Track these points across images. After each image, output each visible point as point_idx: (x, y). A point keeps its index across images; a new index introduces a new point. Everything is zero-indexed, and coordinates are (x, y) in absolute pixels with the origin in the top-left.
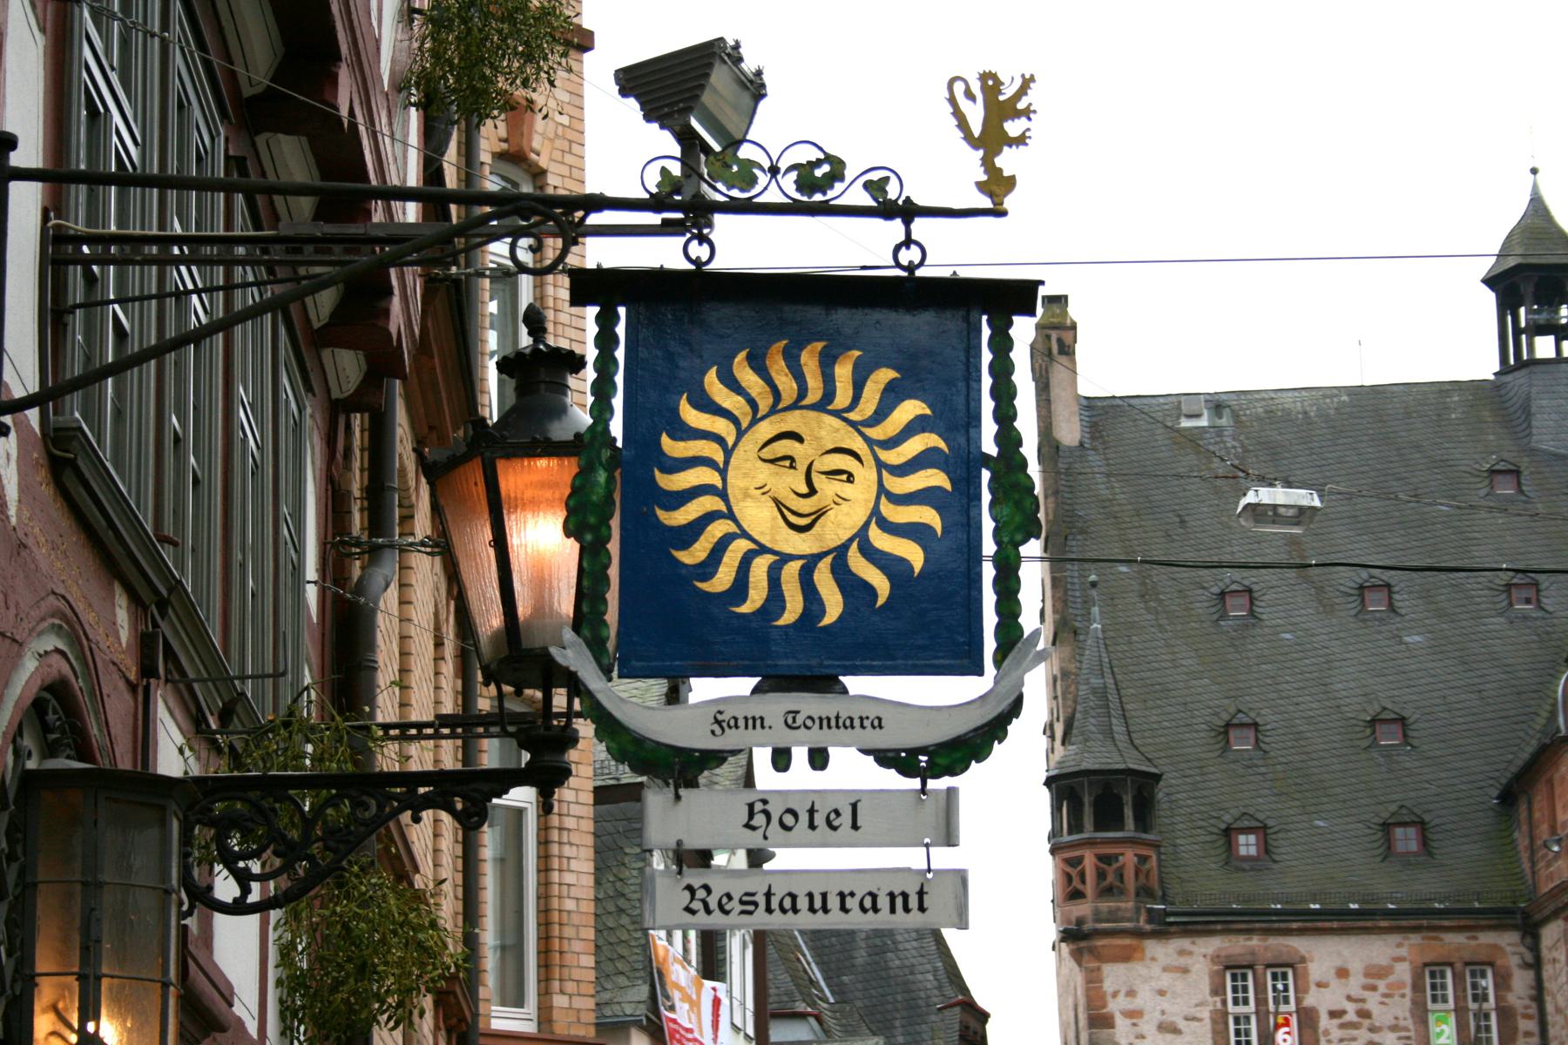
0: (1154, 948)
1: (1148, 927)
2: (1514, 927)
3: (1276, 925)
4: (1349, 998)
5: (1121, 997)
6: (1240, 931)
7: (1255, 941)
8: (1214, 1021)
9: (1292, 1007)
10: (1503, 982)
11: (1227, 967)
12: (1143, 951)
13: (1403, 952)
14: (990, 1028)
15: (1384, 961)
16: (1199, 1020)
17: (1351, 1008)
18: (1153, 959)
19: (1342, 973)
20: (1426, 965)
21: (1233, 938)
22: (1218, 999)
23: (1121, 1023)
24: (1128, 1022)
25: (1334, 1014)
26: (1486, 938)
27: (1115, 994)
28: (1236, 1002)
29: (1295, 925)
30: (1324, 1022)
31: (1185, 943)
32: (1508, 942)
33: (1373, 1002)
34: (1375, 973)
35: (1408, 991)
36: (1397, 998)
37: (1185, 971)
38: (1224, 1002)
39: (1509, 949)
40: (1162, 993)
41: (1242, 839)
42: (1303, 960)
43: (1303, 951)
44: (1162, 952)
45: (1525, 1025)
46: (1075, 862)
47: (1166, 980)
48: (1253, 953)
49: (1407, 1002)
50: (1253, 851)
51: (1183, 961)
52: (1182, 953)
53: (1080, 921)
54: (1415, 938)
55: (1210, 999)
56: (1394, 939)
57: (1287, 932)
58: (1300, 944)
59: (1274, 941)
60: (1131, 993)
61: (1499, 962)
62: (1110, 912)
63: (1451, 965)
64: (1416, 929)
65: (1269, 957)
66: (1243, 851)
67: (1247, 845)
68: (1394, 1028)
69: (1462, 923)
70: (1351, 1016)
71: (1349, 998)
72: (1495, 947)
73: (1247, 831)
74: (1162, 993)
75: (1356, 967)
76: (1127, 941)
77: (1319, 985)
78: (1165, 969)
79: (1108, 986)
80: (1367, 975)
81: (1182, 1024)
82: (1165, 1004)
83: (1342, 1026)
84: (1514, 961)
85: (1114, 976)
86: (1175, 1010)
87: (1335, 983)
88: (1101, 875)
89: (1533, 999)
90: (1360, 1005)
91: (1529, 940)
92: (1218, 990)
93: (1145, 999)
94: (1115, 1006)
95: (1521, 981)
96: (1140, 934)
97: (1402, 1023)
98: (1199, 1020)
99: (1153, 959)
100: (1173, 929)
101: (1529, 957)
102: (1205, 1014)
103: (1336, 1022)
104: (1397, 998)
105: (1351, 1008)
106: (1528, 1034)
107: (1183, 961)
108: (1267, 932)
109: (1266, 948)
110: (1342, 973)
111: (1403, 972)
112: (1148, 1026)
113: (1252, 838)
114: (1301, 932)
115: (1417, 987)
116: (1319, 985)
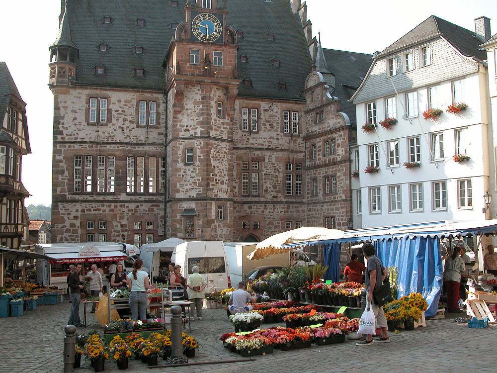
0: (72, 91)
1: (71, 86)
2: (162, 93)
3: (104, 88)
4: (120, 107)
5: (62, 103)
6: (95, 89)
7: (98, 92)
8: (86, 110)
9: (106, 109)
10: (158, 106)
11: (91, 98)
12: (69, 92)
13: (134, 97)
14: (27, 107)
15: (129, 99)
16: (82, 110)
17: (120, 110)
18: (72, 94)
19: (119, 101)
20: (140, 101)
21: (92, 90)
22: (87, 105)
23: (61, 108)
24: (64, 109)
25: (116, 111)
26: (155, 95)
27: (61, 102)
28: (92, 106)
29: (108, 88)
30: (113, 112)
31: (80, 91)
32: (160, 96)
33: (126, 109)
34: (127, 101)
35: (135, 107)
36: (132, 108)
37: (80, 98)
38: (89, 106)
39: (160, 98)
40: (73, 103)
41: (99, 69)
42: (110, 97)
43: (110, 95)
44: (75, 92)
45: (162, 116)
46: (53, 69)
47: (74, 100)
48: (97, 94)
49: (134, 109)
50: (102, 73)
51: (79, 95)
52: (79, 93)
53: (53, 83)
54: (138, 94)
55: (85, 105)
56: (134, 93)
57: (106, 90)
58: (109, 93)
59: (102, 92)
60: (65, 102)
61: (157, 101)
62: (61, 81)
63: (146, 101)
64: (139, 92)
65: (101, 96)
66: (99, 72)
67: (100, 71)
68: (130, 115)
69: (149, 91)
70: (120, 112)
71: (120, 107)
72: (157, 97)
73: (100, 67)
74: (73, 103)
75: (123, 100)
76: (65, 89)
77: (113, 104)
78: (74, 97)
79: (59, 100)
80: (125, 102)
81: (77, 111)
82: (74, 105)
83: (118, 114)
84: (161, 101)
85: (61, 97)
86: (76, 107)
87: (117, 103)
88: (59, 72)
89: (165, 110)
90: (123, 109)
91: (165, 96)
92: (88, 103)
93: (69, 104)
94: (60, 105)
95: (162, 106)
96: (68, 87)
97: (133, 114)
98: (82, 110)
99: (72, 94)
100: (77, 87)
101: (165, 101)
102: (84, 109)
103: (117, 113)
104: (132, 108)
105: (120, 110)
106: (162, 119)
107: (79, 95)
108: (101, 89)
109: (101, 94)
110: (119, 101)
111: (134, 102)
112: (69, 111)
113: (102, 70)
114: (110, 90)
115: (138, 105)
116: (113, 104)
